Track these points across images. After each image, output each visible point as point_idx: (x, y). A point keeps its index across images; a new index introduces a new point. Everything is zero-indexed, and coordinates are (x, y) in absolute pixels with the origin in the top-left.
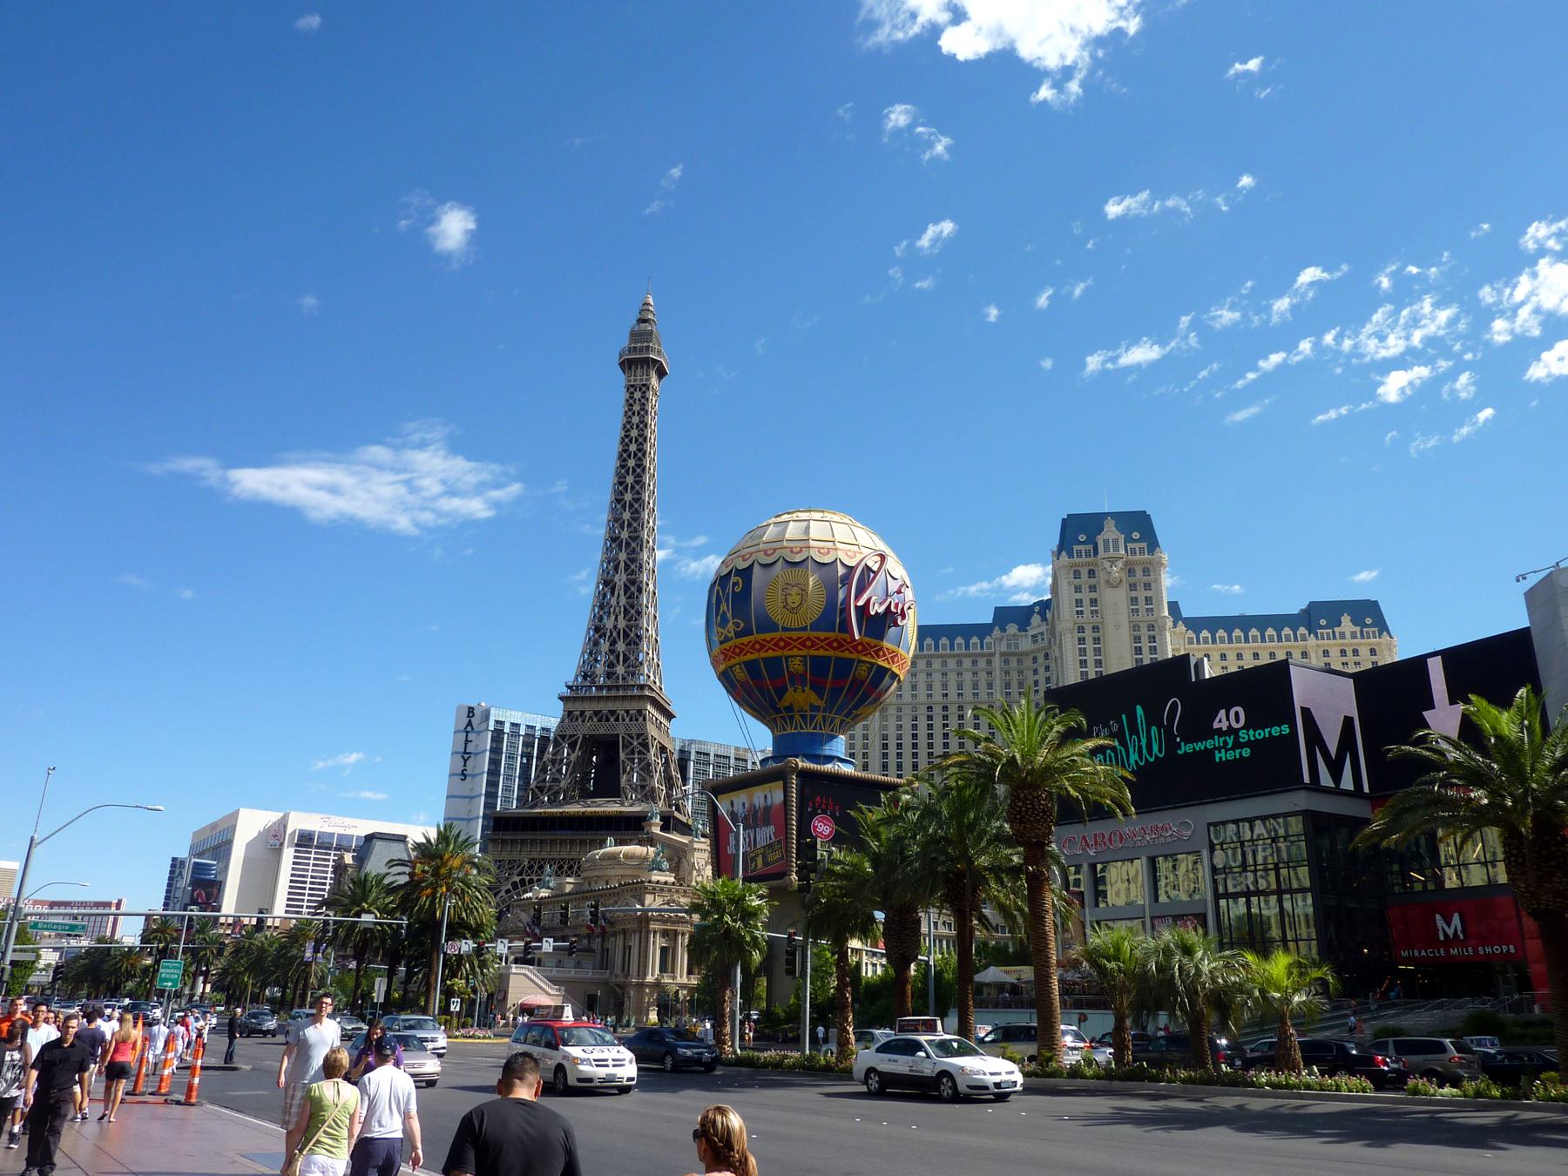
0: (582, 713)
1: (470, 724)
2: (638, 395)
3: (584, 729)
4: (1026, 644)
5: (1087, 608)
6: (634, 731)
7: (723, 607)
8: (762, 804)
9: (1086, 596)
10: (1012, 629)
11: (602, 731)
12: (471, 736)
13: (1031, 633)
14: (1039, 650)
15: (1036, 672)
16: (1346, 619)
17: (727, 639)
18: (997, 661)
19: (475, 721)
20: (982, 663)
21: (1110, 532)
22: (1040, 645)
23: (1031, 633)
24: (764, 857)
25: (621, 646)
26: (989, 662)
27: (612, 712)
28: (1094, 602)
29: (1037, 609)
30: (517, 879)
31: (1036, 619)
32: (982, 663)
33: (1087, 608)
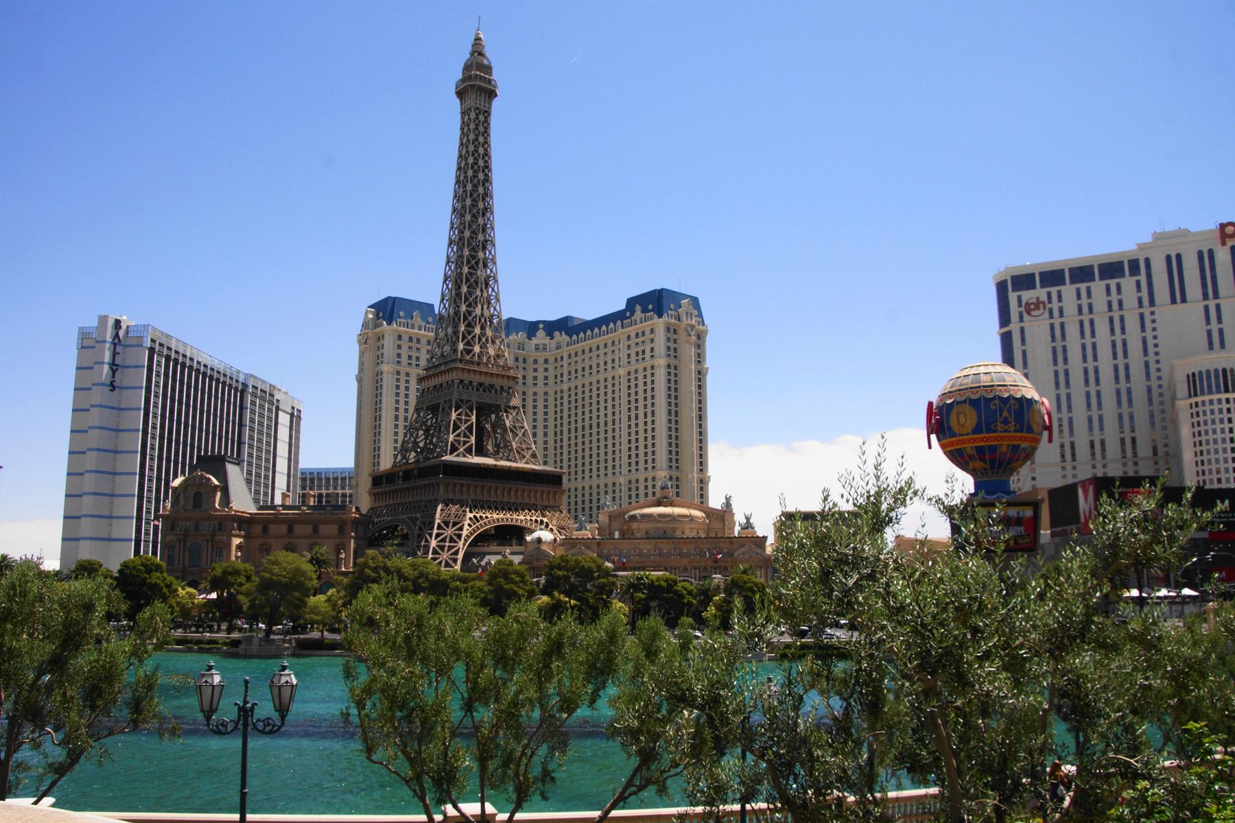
0: (471, 382)
2: (481, 118)
8: (1015, 514)
9: (672, 345)
10: (522, 336)
12: (119, 349)
15: (535, 370)
17: (1006, 431)
19: (121, 333)
23: (534, 341)
24: (1015, 540)
27: (492, 386)
28: (675, 350)
29: (541, 326)
30: (471, 515)
31: (541, 333)
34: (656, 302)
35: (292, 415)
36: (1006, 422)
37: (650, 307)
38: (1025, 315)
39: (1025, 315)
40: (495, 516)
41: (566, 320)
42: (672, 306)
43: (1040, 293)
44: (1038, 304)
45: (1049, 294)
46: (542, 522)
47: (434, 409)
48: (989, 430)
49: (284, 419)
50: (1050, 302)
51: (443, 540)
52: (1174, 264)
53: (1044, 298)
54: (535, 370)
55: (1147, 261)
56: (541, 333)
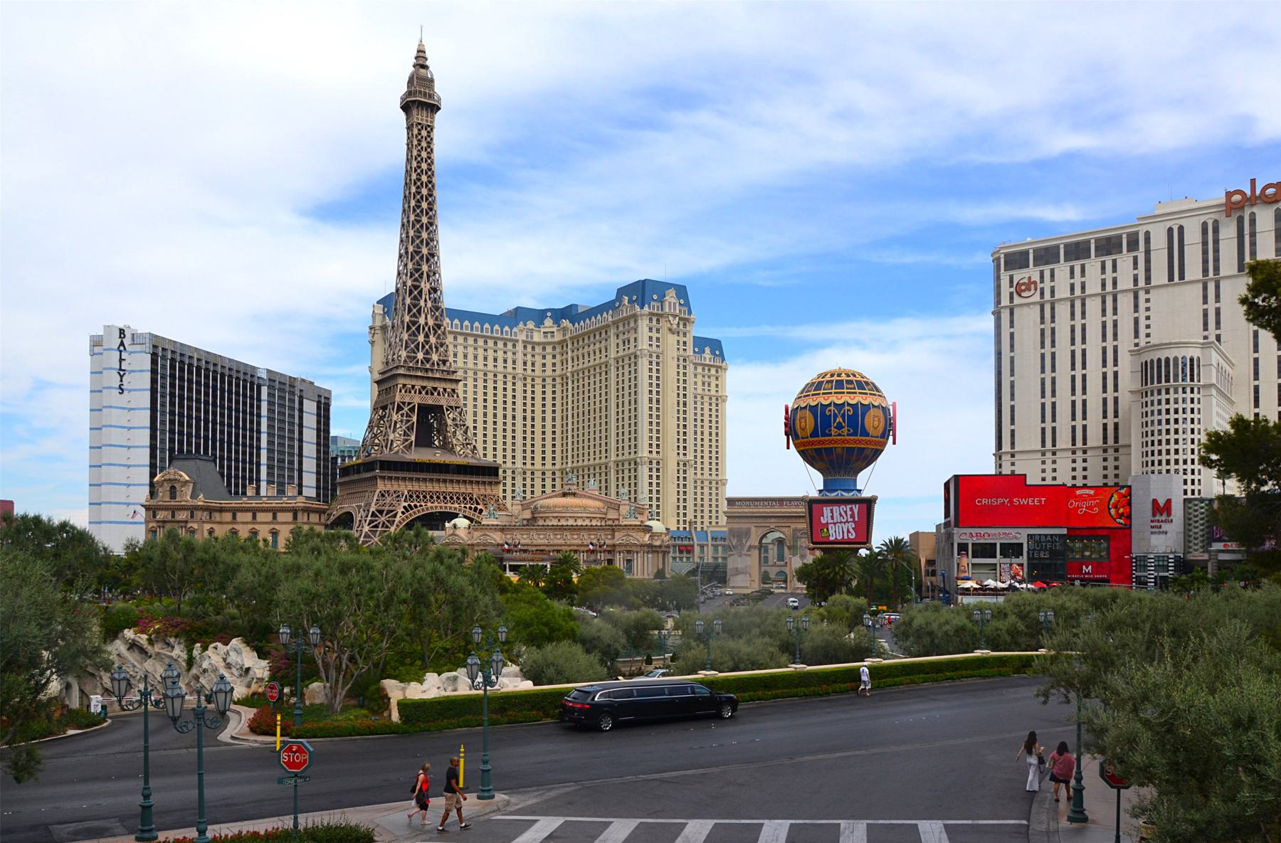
0: (413, 387)
1: (122, 344)
3: (417, 400)
4: (537, 337)
5: (654, 343)
6: (453, 404)
7: (839, 419)
9: (654, 335)
10: (531, 325)
11: (430, 402)
12: (124, 355)
13: (543, 330)
14: (549, 343)
15: (544, 357)
16: (707, 350)
18: (520, 347)
19: (127, 341)
20: (510, 345)
21: (671, 297)
22: (549, 339)
25: (433, 340)
26: (514, 346)
27: (435, 389)
28: (658, 339)
29: (549, 314)
31: (548, 322)
32: (510, 345)
33: (654, 343)
34: (641, 291)
35: (319, 402)
36: (839, 427)
37: (635, 298)
38: (1015, 295)
39: (1015, 295)
40: (429, 504)
41: (571, 307)
42: (655, 297)
43: (1032, 272)
44: (1030, 284)
45: (1042, 273)
46: (476, 509)
47: (384, 408)
48: (824, 435)
49: (310, 407)
50: (1042, 281)
51: (376, 526)
52: (1176, 239)
53: (1036, 277)
54: (544, 357)
55: (1147, 234)
56: (548, 322)
